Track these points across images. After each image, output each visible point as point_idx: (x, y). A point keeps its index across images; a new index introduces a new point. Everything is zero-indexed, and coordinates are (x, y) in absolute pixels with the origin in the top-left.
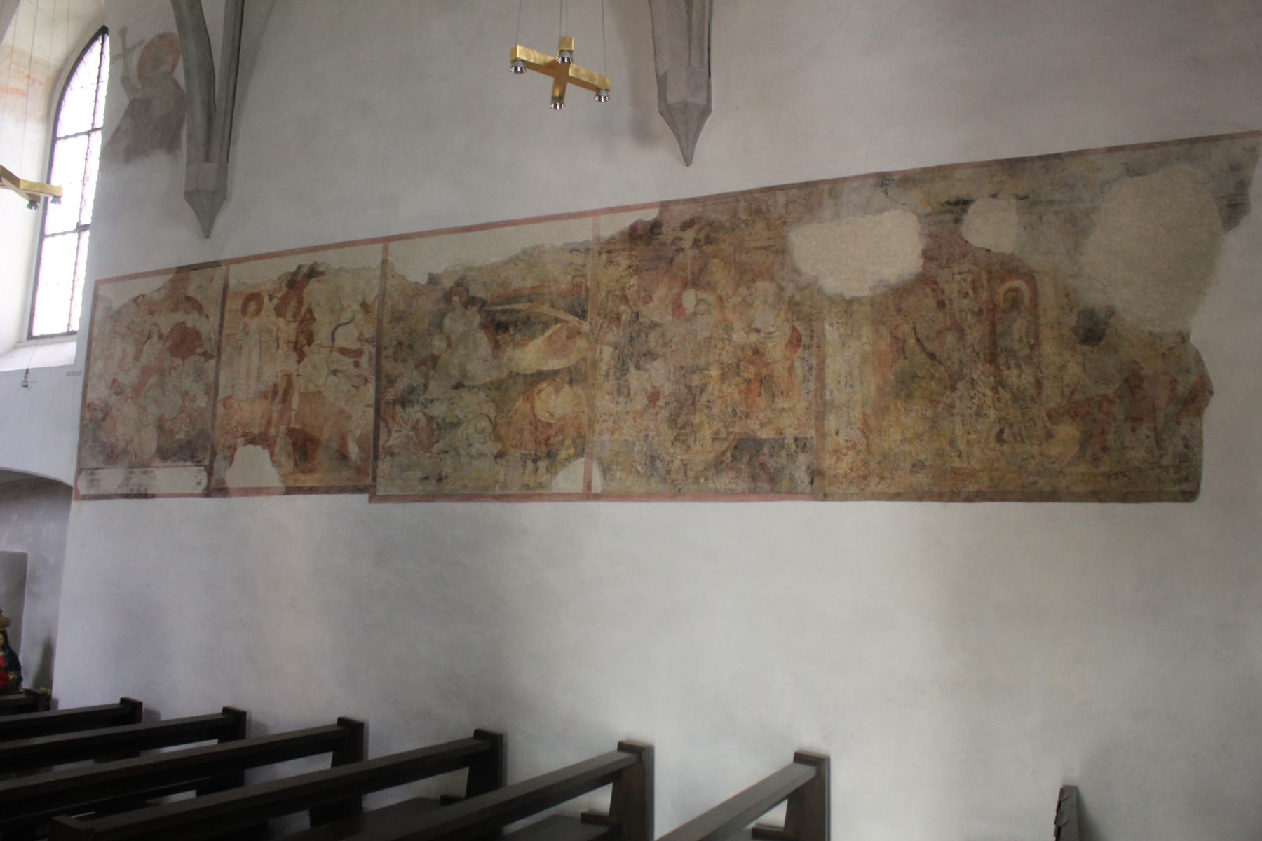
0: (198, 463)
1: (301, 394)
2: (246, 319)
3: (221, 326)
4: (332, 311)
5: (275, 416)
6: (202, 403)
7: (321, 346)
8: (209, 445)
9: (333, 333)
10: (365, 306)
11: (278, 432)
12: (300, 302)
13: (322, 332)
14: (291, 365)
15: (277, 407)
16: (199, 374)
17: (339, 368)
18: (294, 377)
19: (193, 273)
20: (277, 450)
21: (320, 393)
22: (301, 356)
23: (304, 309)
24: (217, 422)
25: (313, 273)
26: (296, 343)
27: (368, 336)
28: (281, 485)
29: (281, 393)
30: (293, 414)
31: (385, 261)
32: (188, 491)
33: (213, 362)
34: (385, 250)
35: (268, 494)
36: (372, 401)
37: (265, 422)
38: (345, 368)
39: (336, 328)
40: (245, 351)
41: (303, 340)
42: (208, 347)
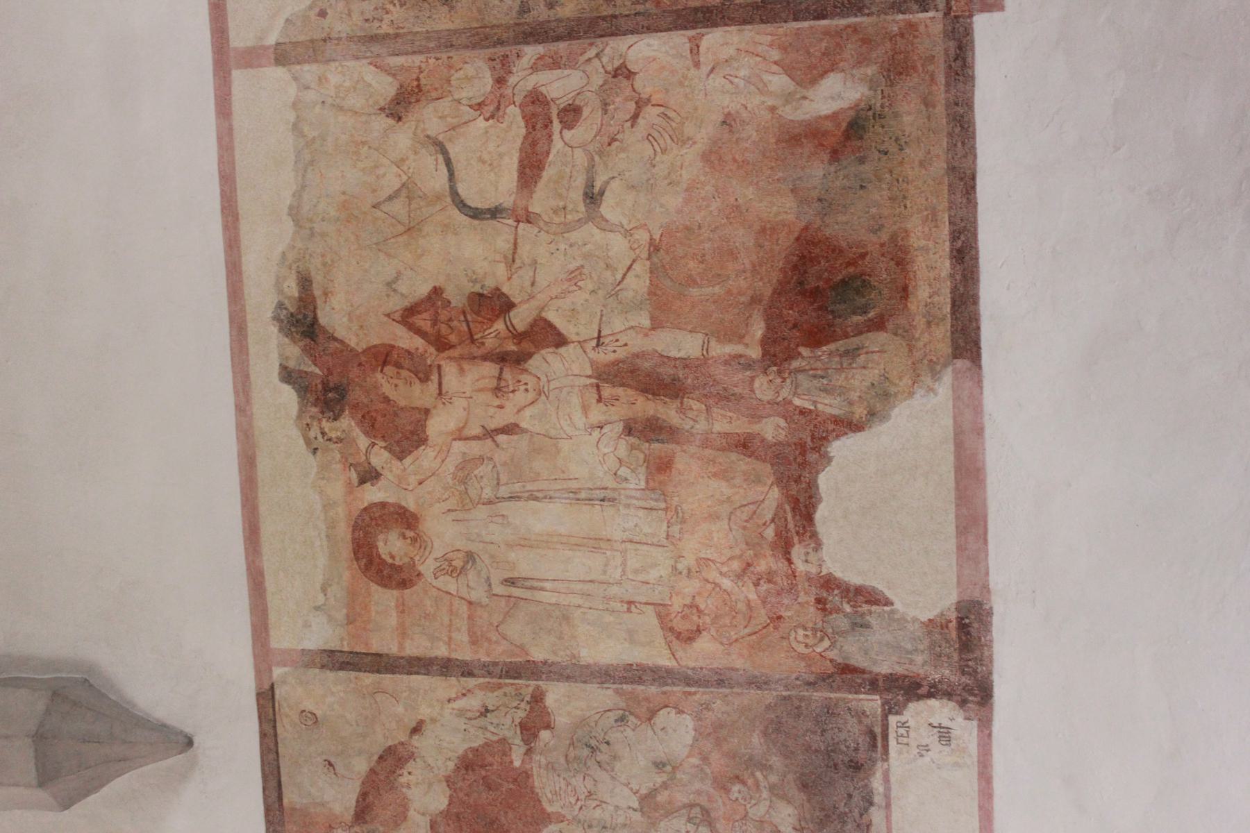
0: (877, 740)
1: (656, 325)
2: (427, 567)
3: (446, 667)
4: (412, 230)
5: (725, 423)
6: (677, 733)
7: (511, 260)
8: (818, 695)
9: (476, 214)
10: (400, 105)
11: (774, 403)
12: (384, 357)
13: (464, 258)
14: (561, 368)
15: (700, 420)
16: (590, 749)
17: (580, 181)
18: (605, 356)
19: (290, 797)
20: (830, 406)
21: (654, 247)
22: (544, 335)
23: (406, 340)
24: (739, 662)
25: (303, 322)
26: (502, 359)
27: (487, 82)
28: (947, 377)
29: (648, 389)
30: (721, 350)
31: (282, 56)
32: (967, 779)
33: (555, 694)
34: (251, 57)
35: (979, 431)
36: (680, 39)
37: (743, 464)
38: (580, 157)
39: (461, 205)
40: (525, 564)
41: (494, 334)
42: (506, 725)
